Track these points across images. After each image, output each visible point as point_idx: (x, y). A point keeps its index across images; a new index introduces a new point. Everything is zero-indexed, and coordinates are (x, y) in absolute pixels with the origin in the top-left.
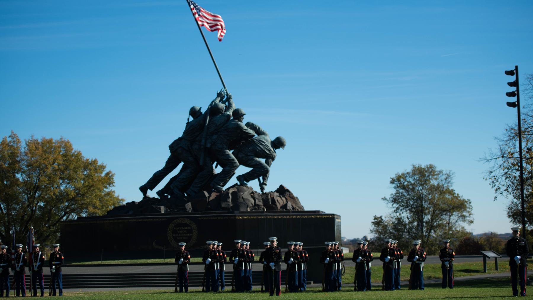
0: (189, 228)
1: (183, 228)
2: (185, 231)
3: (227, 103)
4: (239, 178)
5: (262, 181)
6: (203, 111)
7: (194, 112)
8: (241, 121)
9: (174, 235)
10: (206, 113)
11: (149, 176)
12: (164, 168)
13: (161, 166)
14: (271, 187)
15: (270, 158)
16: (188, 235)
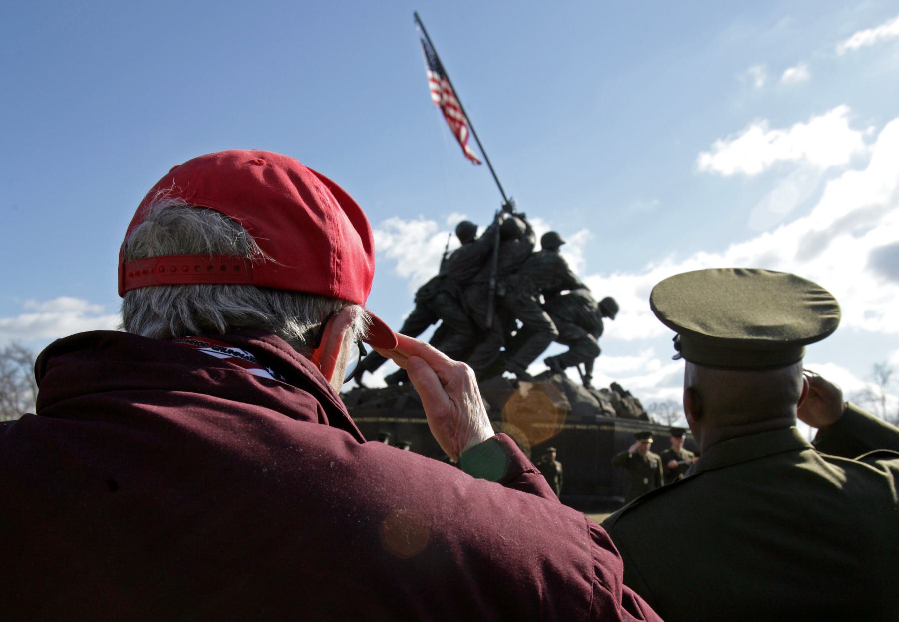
4: (548, 362)
5: (584, 373)
14: (600, 381)
15: (598, 330)
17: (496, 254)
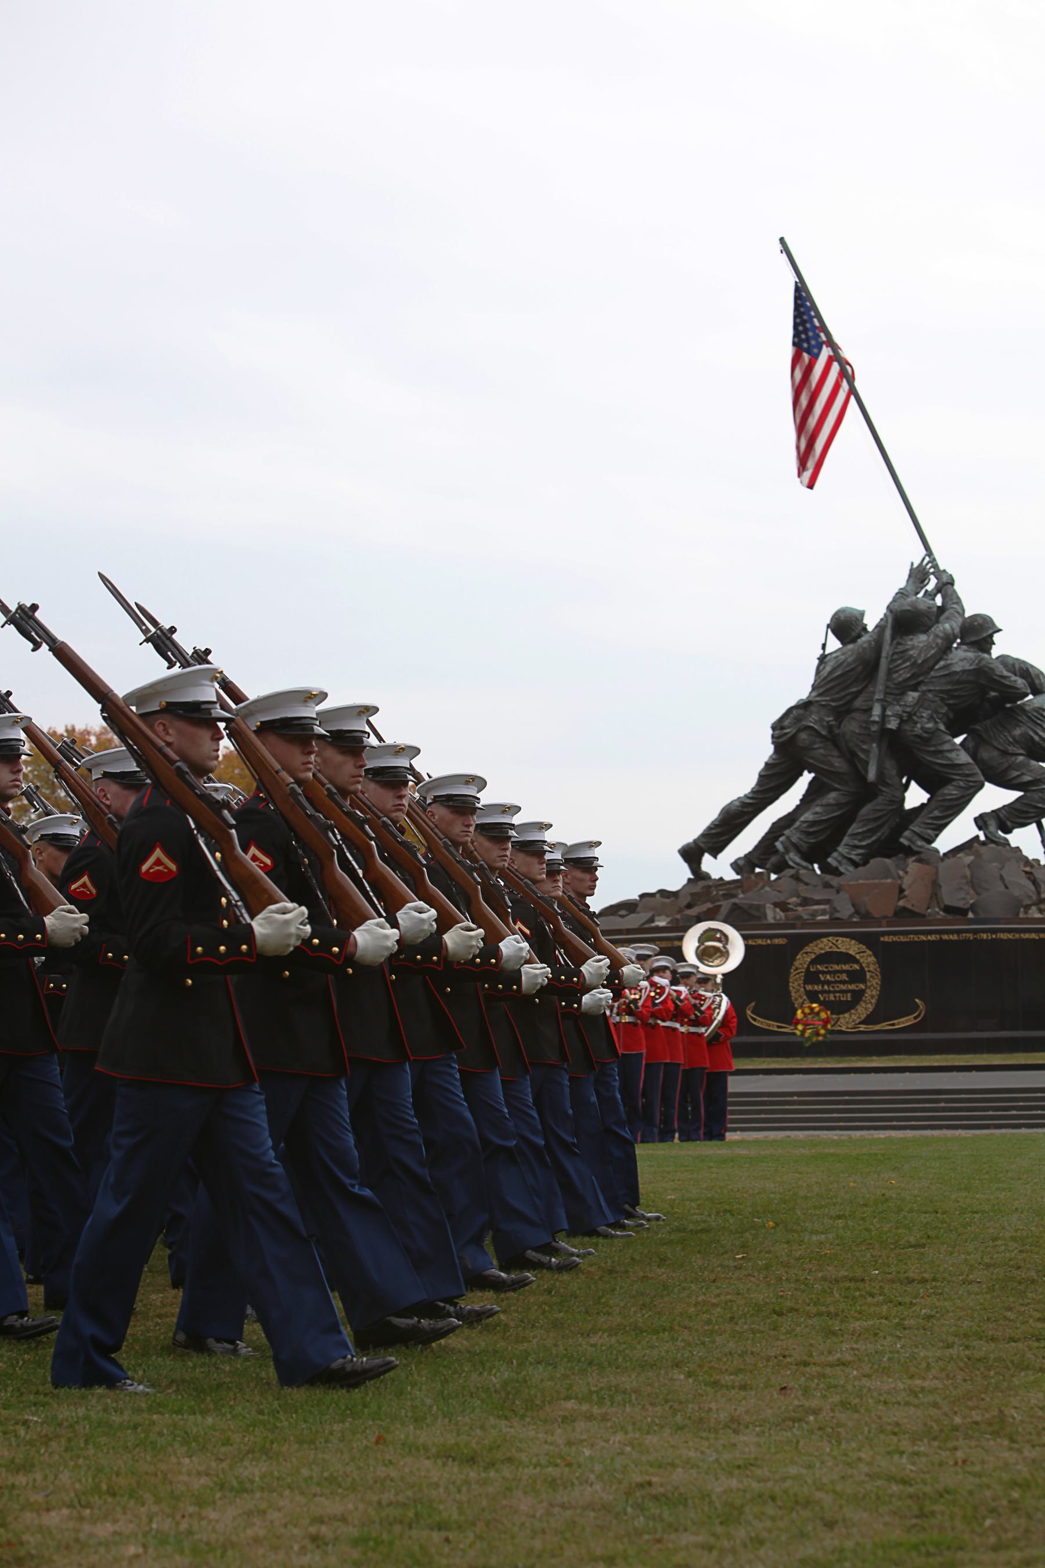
0: (856, 967)
1: (836, 967)
2: (844, 977)
3: (939, 600)
4: (981, 821)
6: (871, 622)
7: (845, 625)
8: (990, 653)
9: (809, 987)
10: (880, 627)
11: (708, 815)
12: (753, 791)
13: (743, 783)
16: (852, 987)
17: (884, 664)
